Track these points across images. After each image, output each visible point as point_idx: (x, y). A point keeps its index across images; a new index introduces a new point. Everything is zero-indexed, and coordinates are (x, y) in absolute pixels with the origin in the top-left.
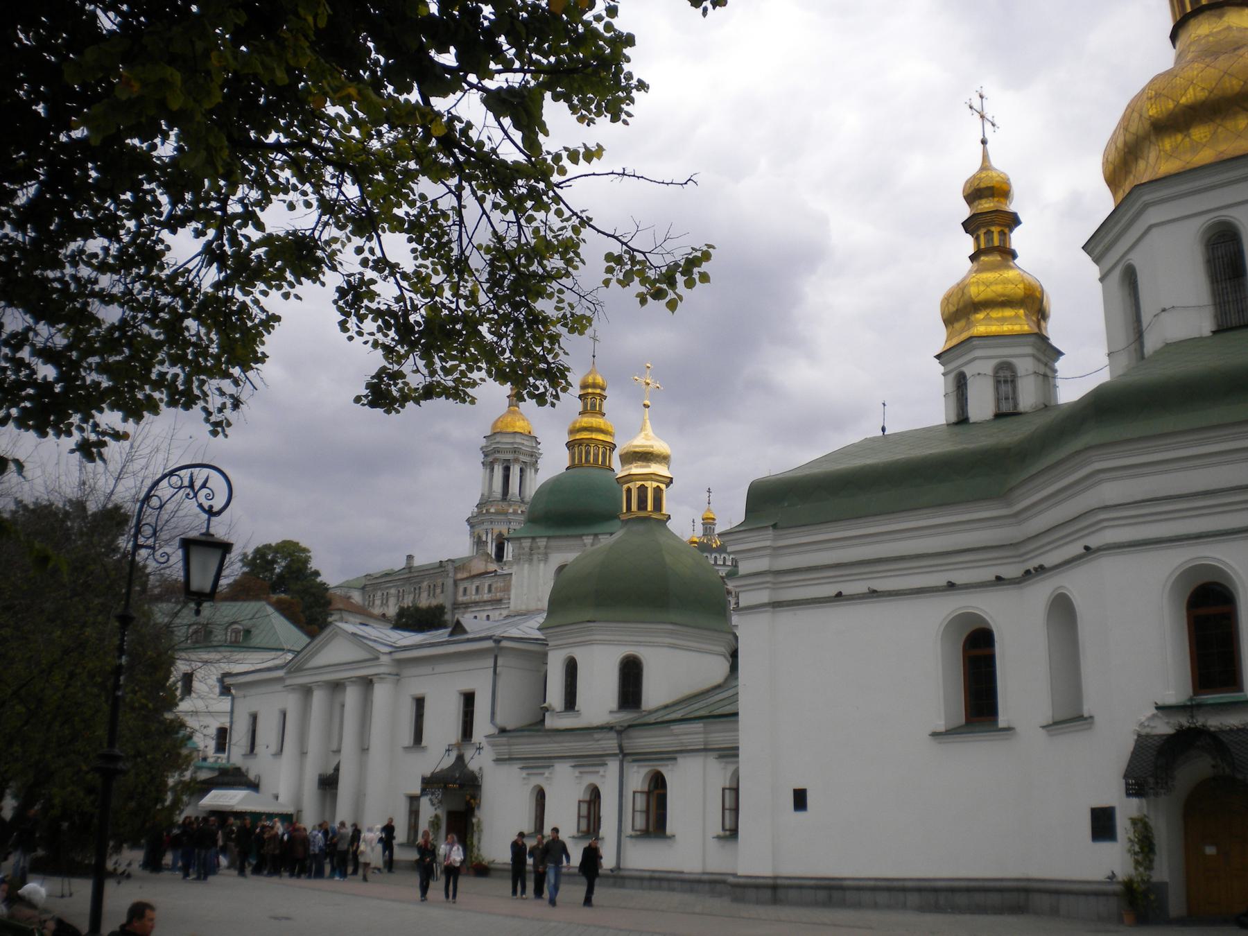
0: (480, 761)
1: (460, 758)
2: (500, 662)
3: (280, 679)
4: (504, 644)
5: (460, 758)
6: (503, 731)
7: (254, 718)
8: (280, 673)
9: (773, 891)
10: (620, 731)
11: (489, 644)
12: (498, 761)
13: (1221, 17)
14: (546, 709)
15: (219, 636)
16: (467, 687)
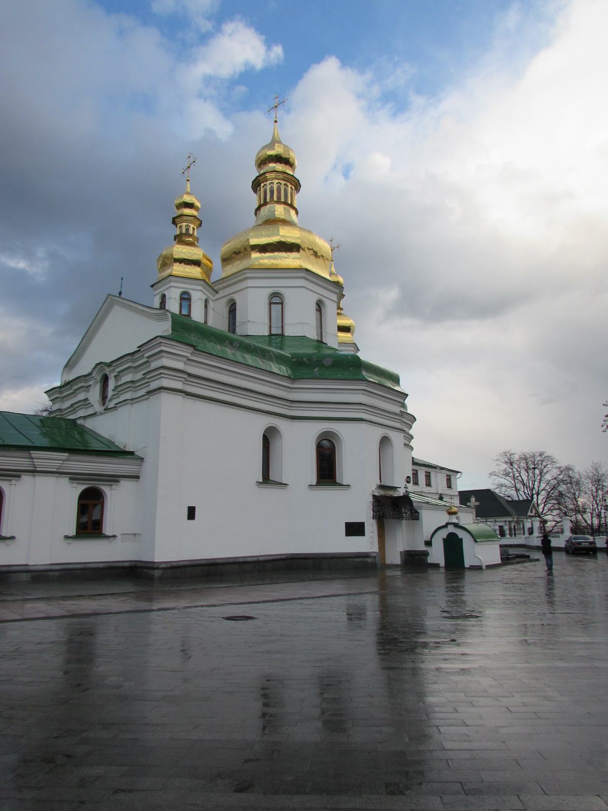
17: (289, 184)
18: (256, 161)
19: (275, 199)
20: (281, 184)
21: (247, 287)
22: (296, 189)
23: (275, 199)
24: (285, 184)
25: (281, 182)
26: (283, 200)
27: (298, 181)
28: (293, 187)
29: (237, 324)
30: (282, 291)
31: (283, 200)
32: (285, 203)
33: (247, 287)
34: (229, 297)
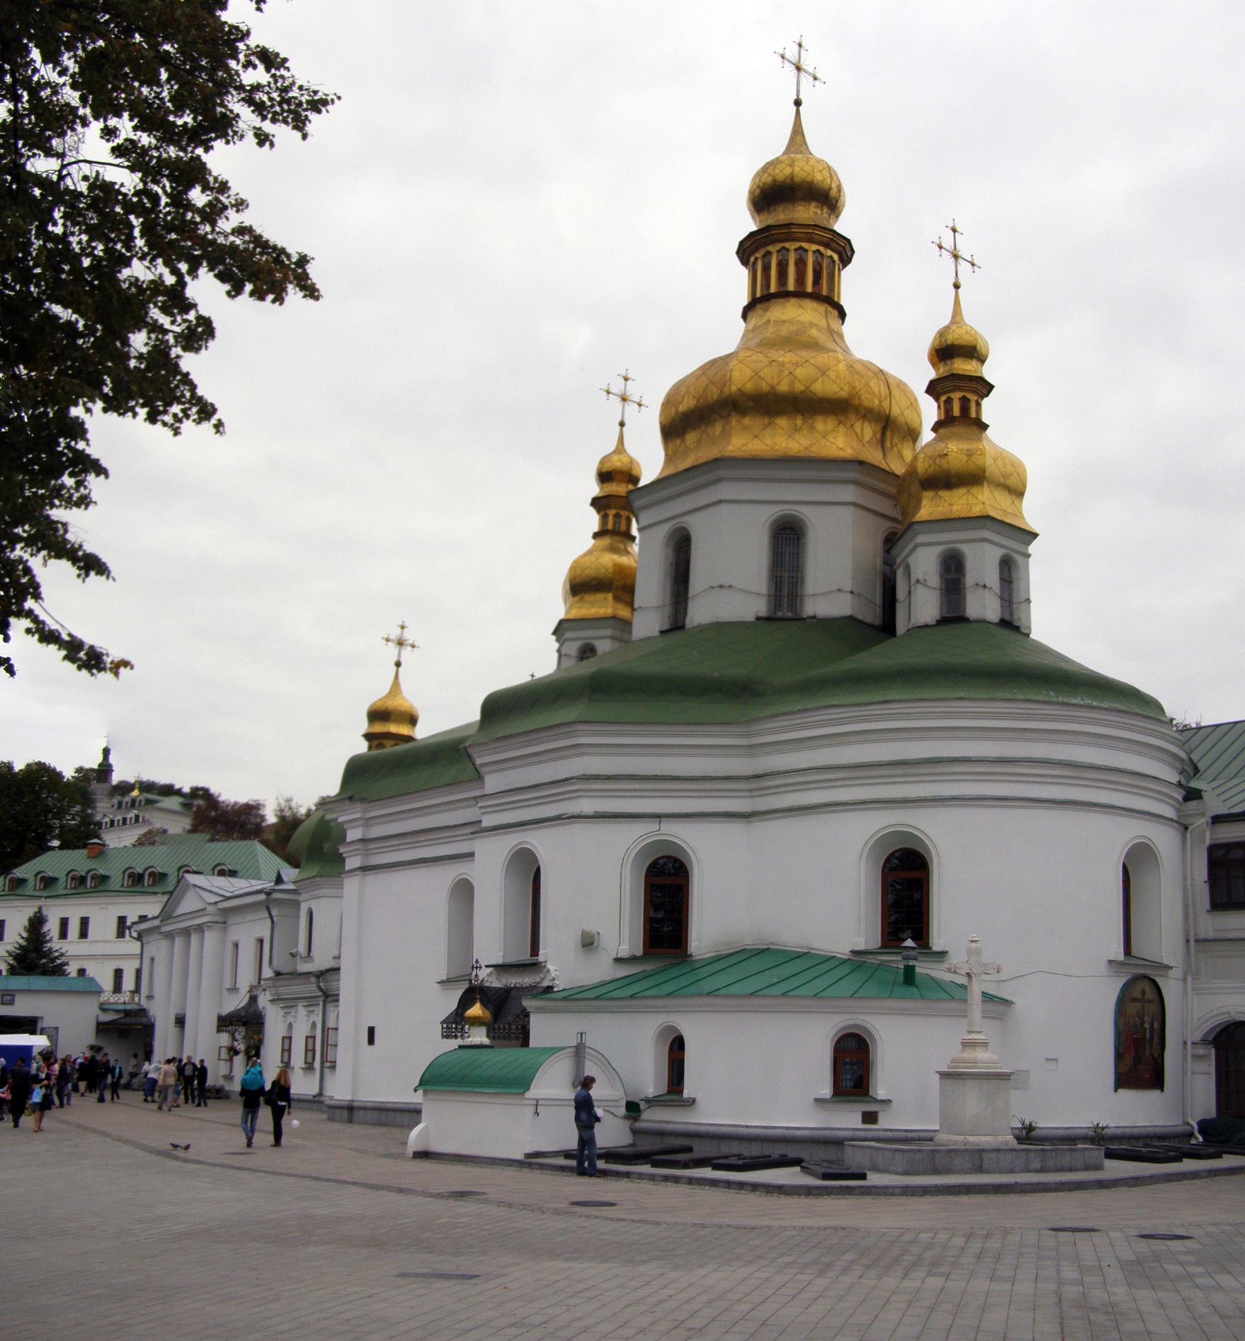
0: (264, 1001)
1: (253, 999)
2: (274, 913)
3: (158, 927)
4: (276, 895)
5: (253, 999)
6: (278, 974)
7: (152, 960)
8: (156, 923)
9: (350, 1112)
10: (320, 975)
11: (262, 897)
12: (272, 1001)
13: (766, 310)
14: (293, 955)
15: (115, 883)
16: (259, 935)
17: (822, 249)
18: (751, 193)
19: (791, 286)
20: (806, 251)
21: (720, 502)
22: (841, 259)
23: (791, 286)
24: (818, 251)
25: (804, 245)
26: (809, 289)
27: (849, 241)
28: (836, 257)
29: (692, 592)
30: (806, 513)
31: (809, 289)
32: (816, 297)
33: (720, 502)
34: (676, 521)
